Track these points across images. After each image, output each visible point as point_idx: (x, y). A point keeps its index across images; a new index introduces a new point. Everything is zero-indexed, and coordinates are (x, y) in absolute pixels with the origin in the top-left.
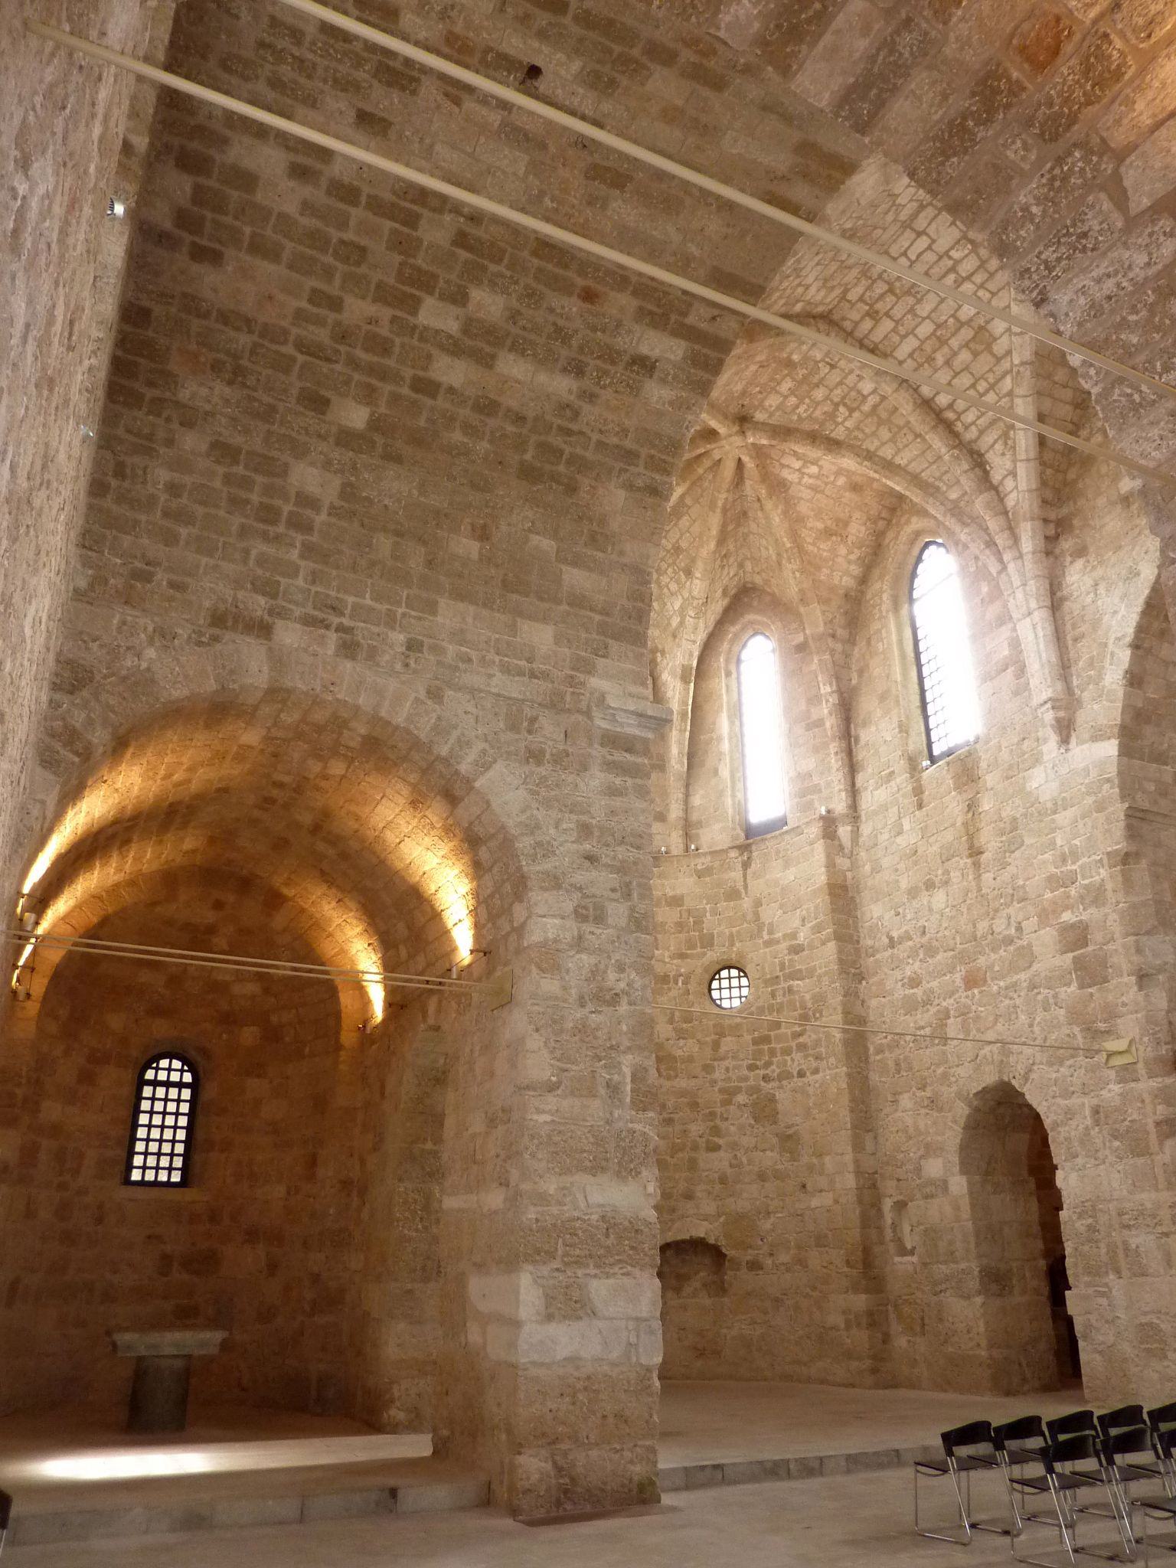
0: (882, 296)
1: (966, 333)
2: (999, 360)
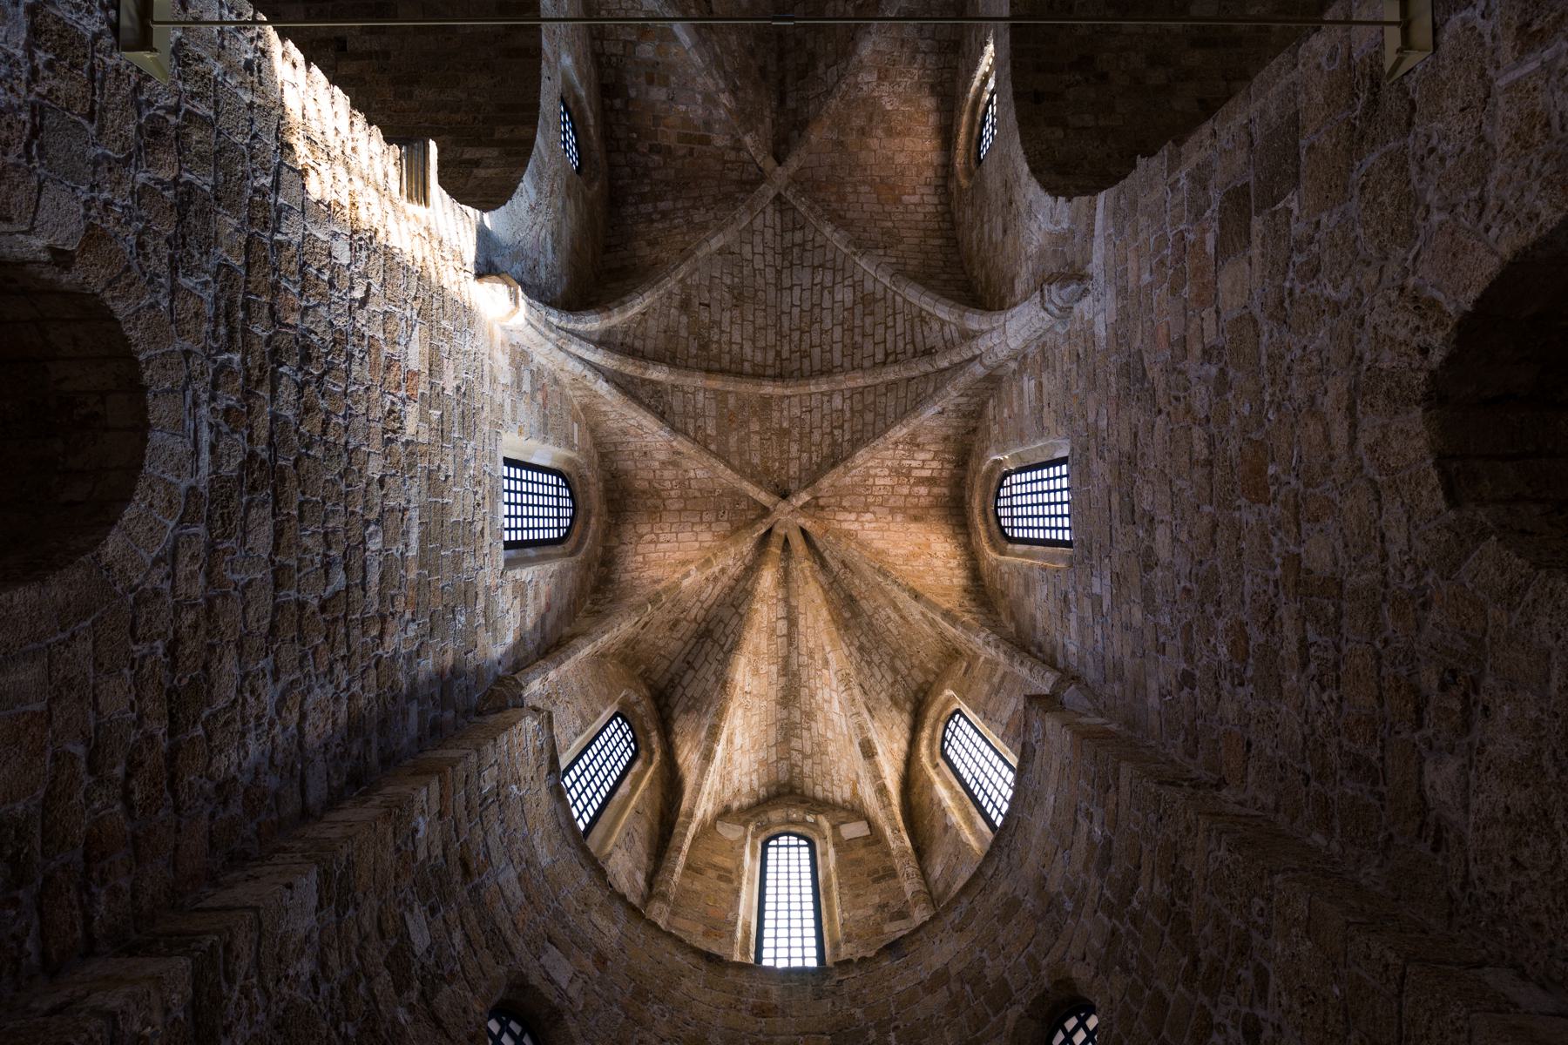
0: (801, 340)
1: (859, 309)
2: (884, 298)
